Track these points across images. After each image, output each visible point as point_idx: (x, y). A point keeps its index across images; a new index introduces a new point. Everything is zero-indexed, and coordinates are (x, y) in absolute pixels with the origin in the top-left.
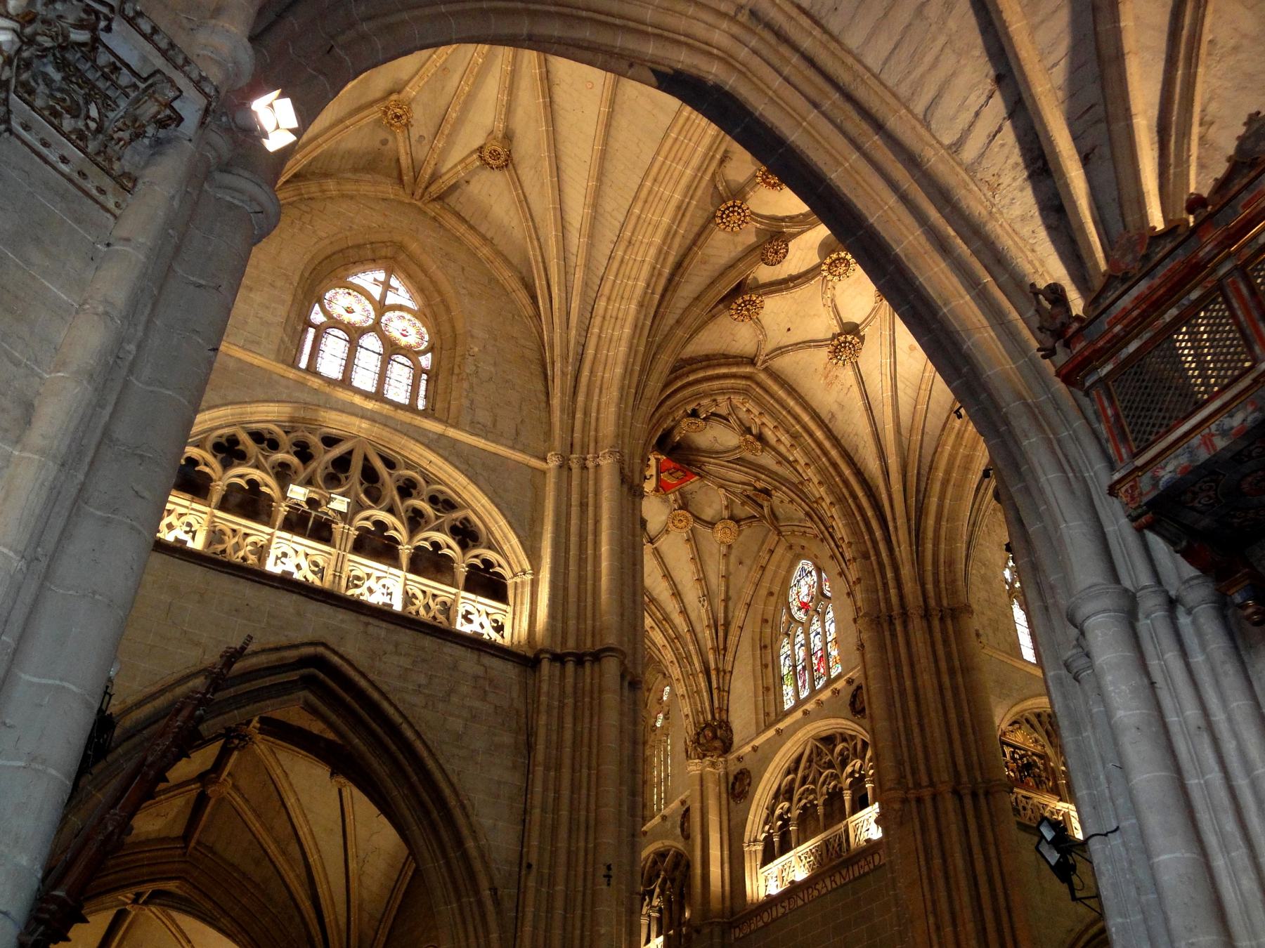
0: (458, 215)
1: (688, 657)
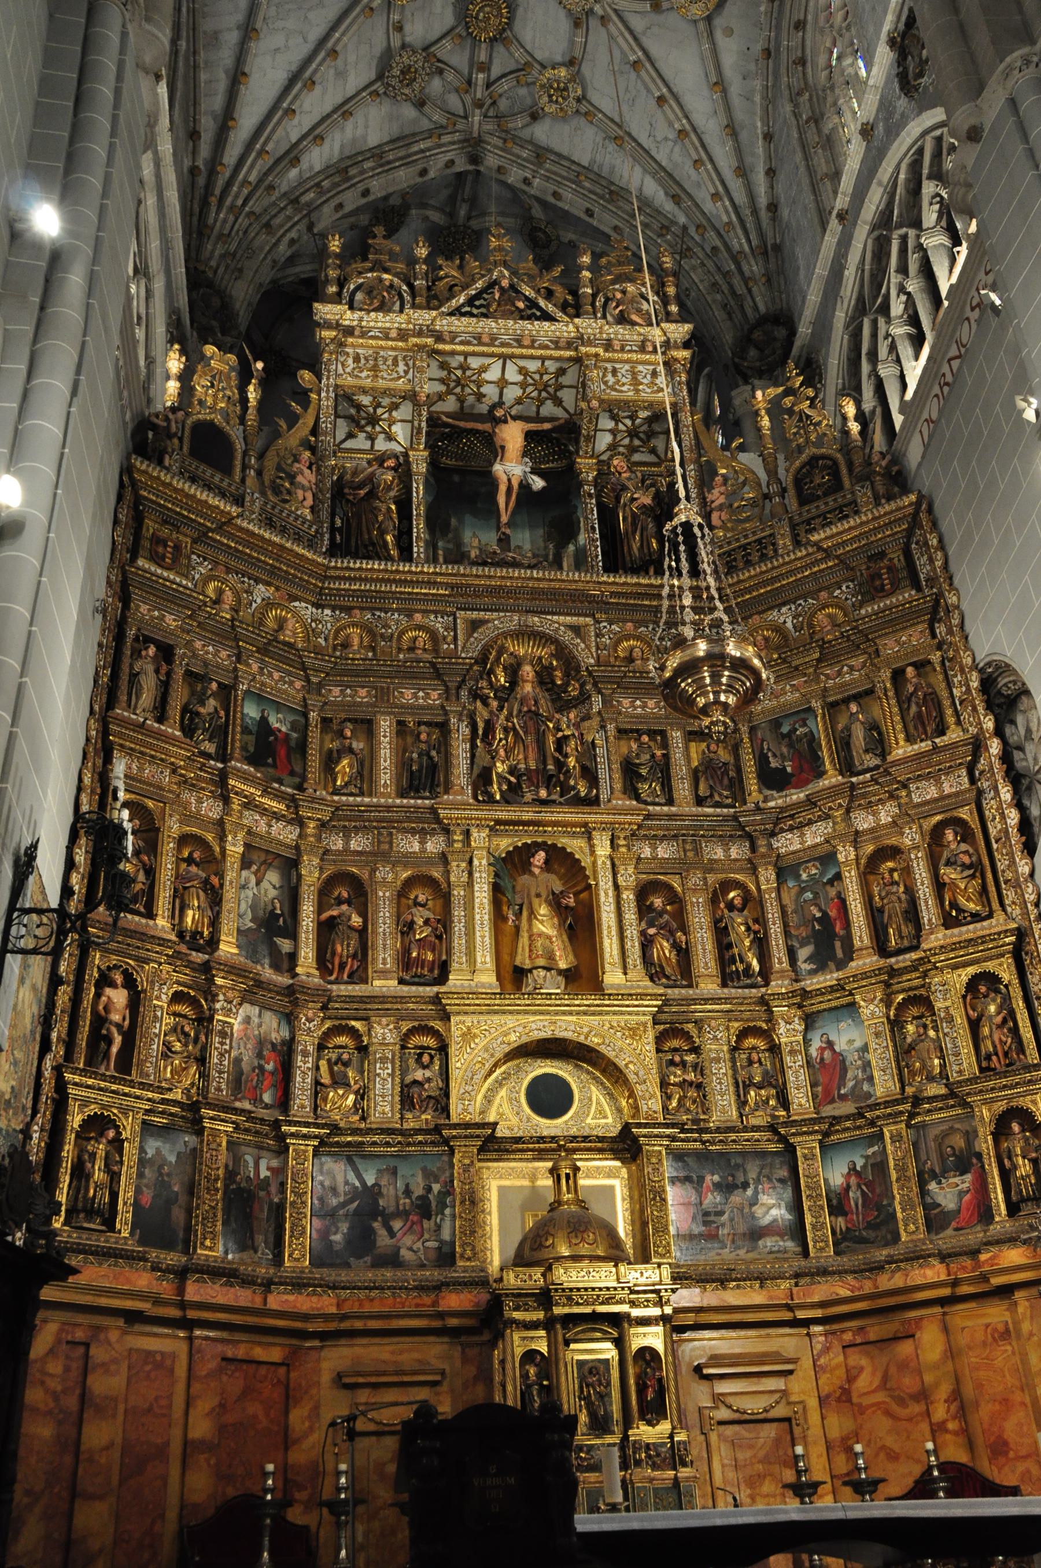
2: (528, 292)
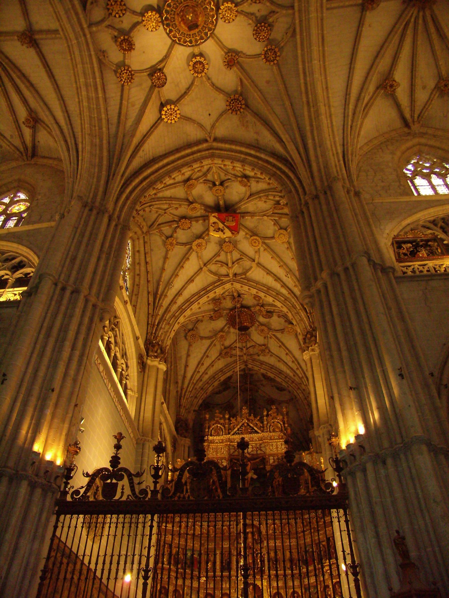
0: (44, 157)
2: (251, 425)
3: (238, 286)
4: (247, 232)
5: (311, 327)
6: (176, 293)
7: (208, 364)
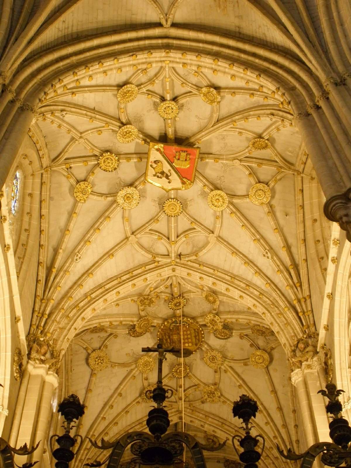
1: (274, 304)
3: (182, 272)
4: (207, 183)
5: (304, 332)
6: (82, 272)
7: (120, 410)
